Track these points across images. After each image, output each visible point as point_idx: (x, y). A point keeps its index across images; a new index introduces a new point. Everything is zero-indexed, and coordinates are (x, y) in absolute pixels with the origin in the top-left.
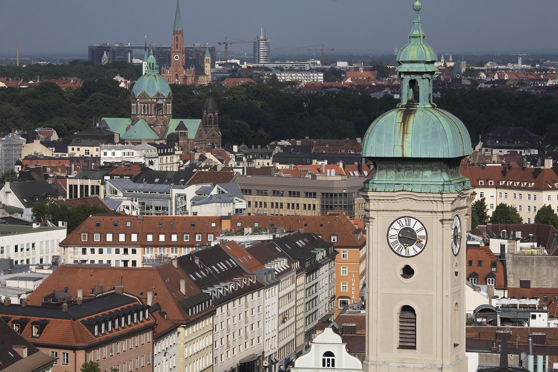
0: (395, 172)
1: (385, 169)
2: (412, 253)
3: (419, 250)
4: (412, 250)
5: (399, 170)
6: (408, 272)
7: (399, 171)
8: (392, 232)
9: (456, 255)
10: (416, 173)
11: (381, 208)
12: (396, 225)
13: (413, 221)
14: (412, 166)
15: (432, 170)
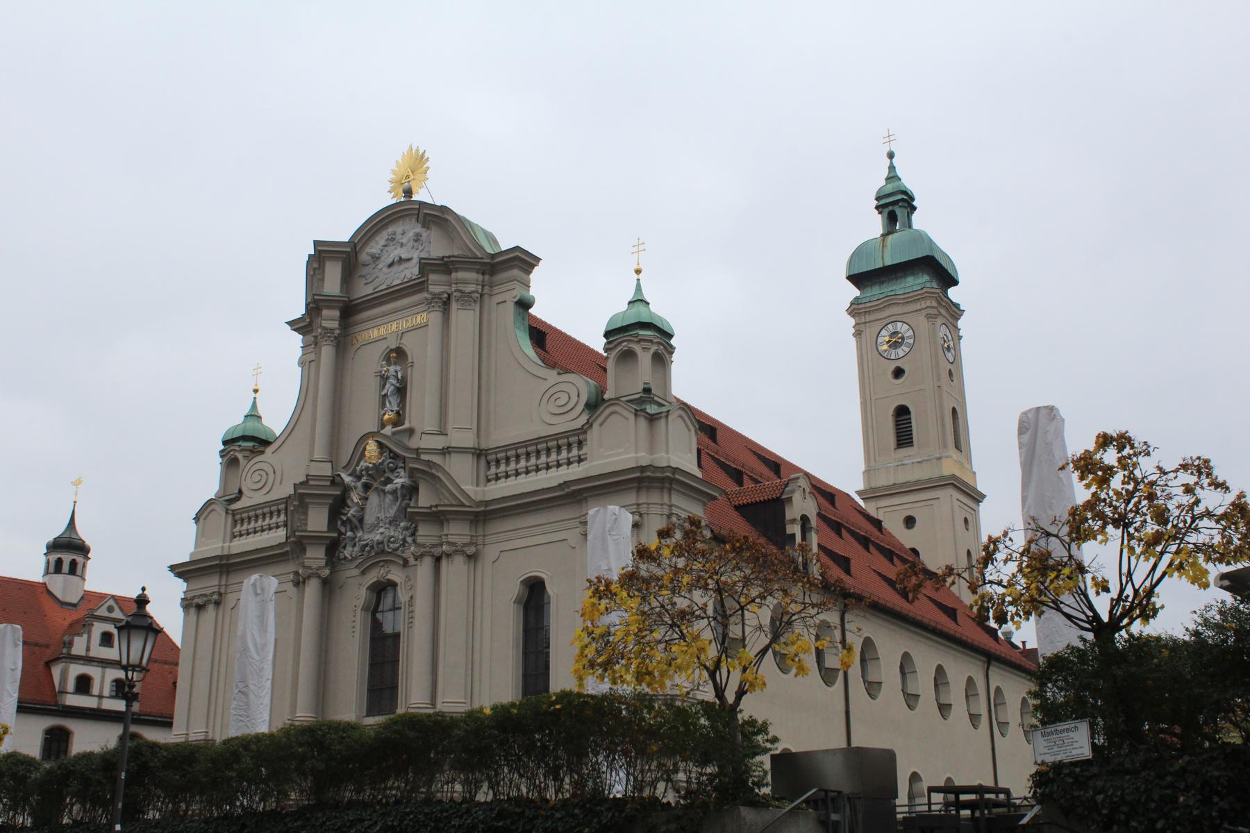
0: (880, 286)
1: (869, 286)
2: (901, 354)
3: (907, 350)
4: (901, 352)
5: (882, 283)
6: (898, 373)
7: (882, 284)
8: (880, 340)
9: (952, 363)
10: (898, 281)
11: (867, 320)
12: (884, 332)
13: (899, 324)
14: (894, 276)
15: (914, 276)
